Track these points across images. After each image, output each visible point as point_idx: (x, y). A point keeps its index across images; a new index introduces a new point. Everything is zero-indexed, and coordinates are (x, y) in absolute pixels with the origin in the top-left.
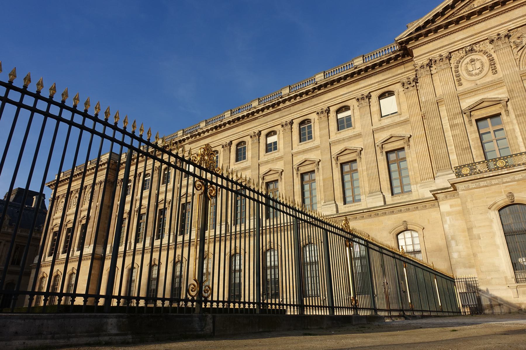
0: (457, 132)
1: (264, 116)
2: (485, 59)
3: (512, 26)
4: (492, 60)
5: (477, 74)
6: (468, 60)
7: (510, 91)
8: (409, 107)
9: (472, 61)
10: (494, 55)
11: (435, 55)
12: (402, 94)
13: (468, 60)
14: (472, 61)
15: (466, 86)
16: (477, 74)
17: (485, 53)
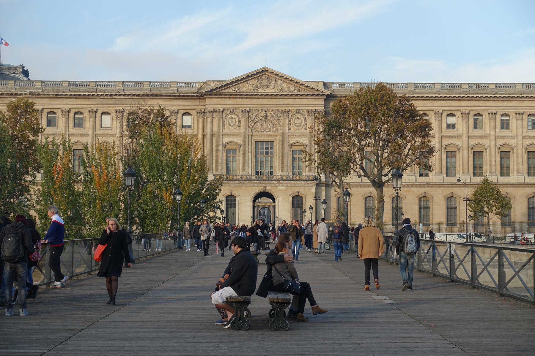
0: (218, 154)
1: (101, 98)
2: (237, 119)
3: (251, 108)
4: (239, 121)
5: (232, 126)
6: (230, 116)
7: (243, 141)
8: (198, 128)
9: (232, 118)
10: (241, 119)
11: (217, 108)
12: (196, 117)
13: (230, 116)
14: (232, 118)
15: (226, 131)
16: (232, 126)
17: (238, 116)
